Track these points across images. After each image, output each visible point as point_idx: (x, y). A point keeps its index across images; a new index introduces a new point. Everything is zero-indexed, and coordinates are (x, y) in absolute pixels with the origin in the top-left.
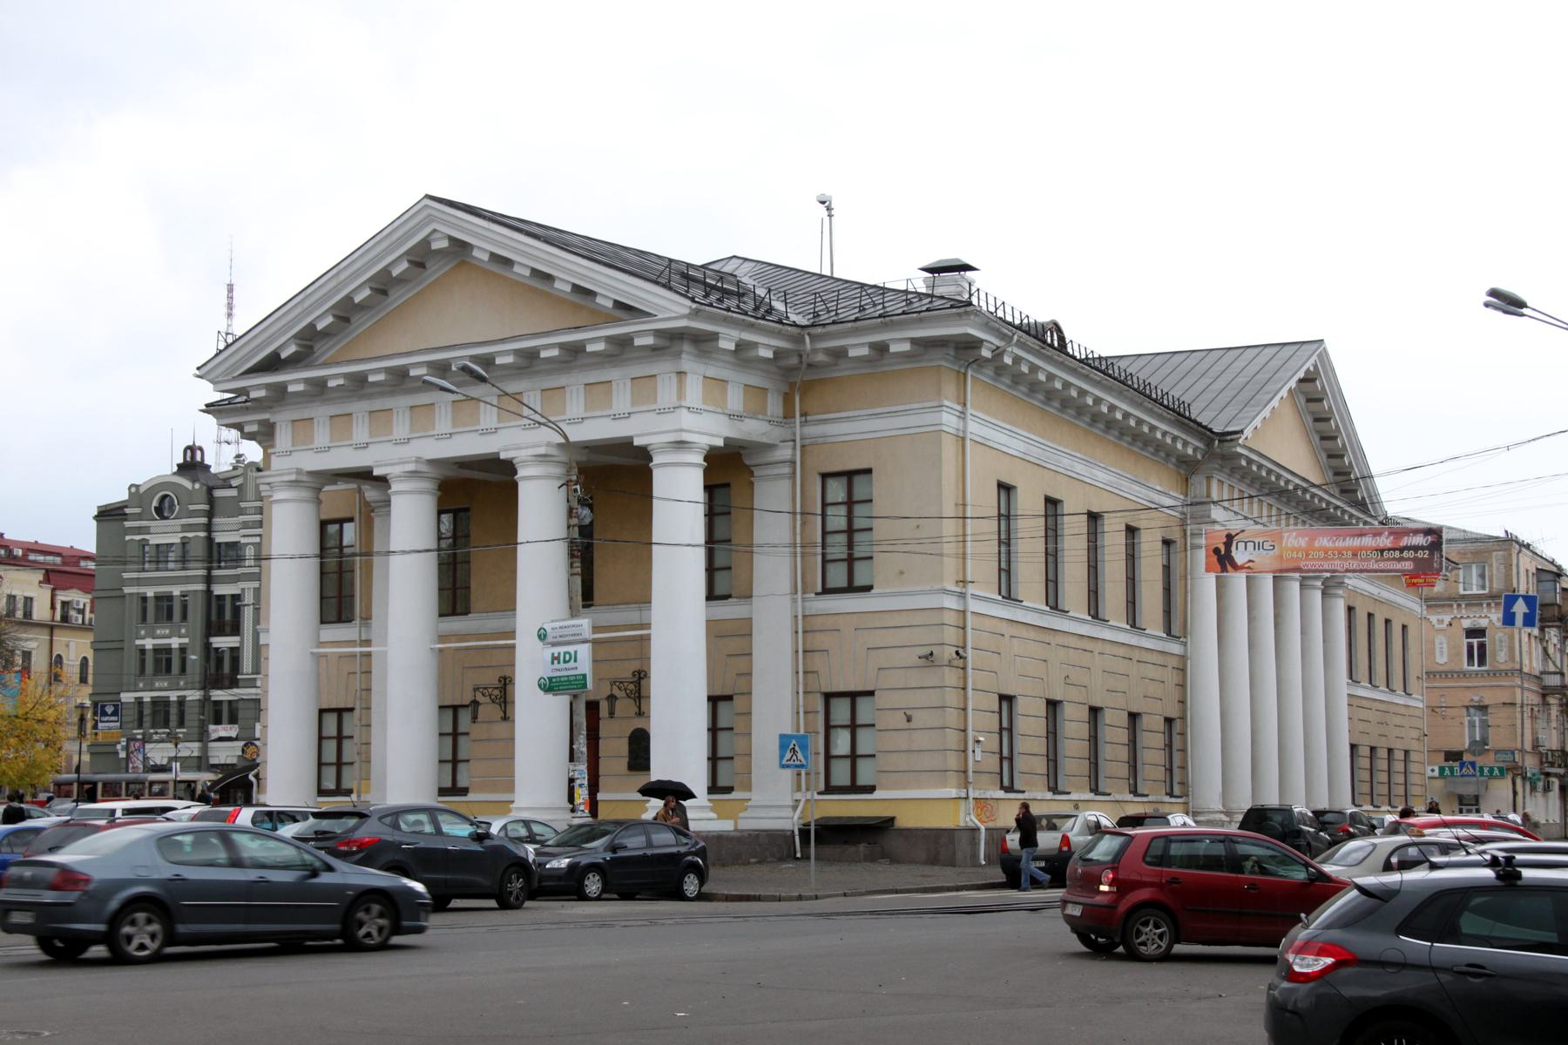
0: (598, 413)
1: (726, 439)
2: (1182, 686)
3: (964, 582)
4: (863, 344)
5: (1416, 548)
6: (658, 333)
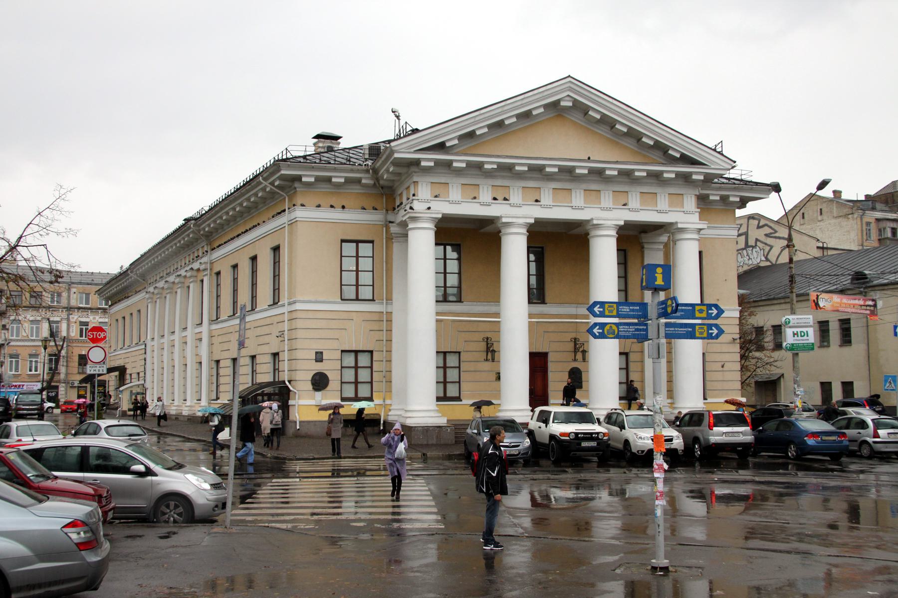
5: (870, 306)
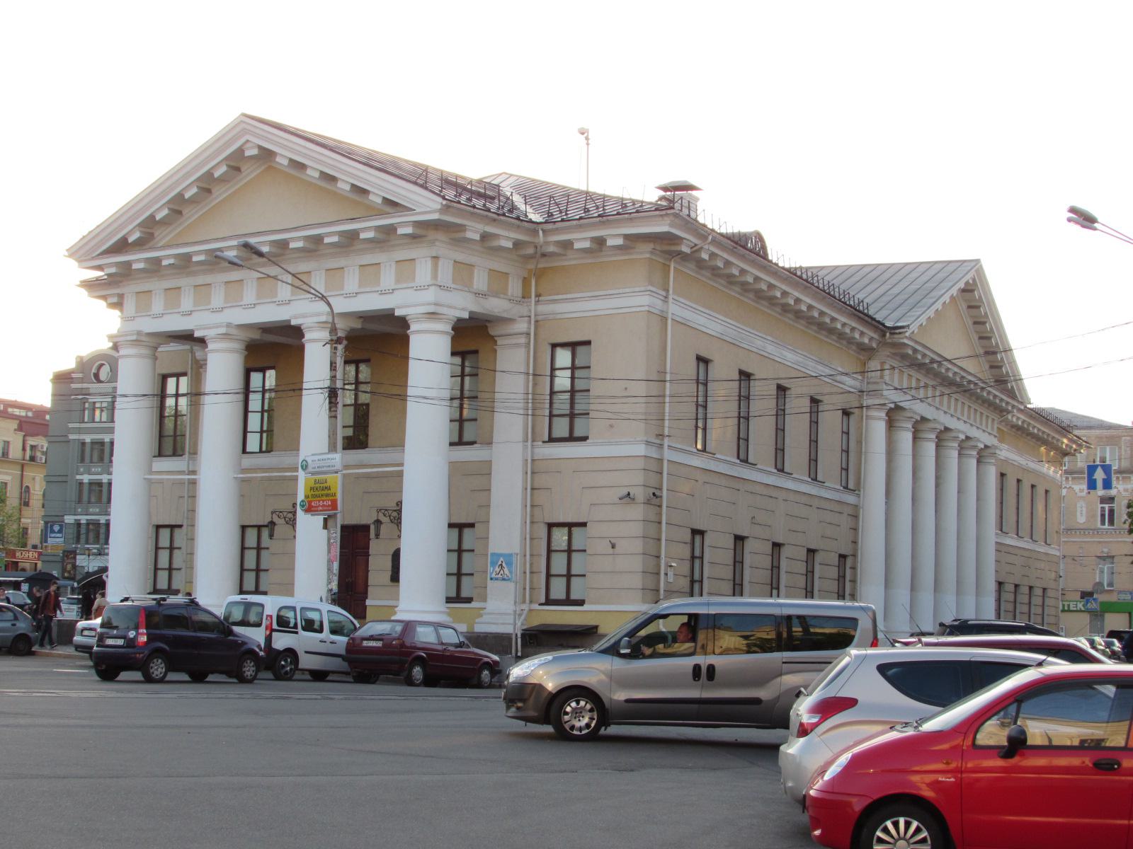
0: (368, 290)
1: (471, 313)
2: (855, 529)
3: (661, 436)
6: (418, 224)
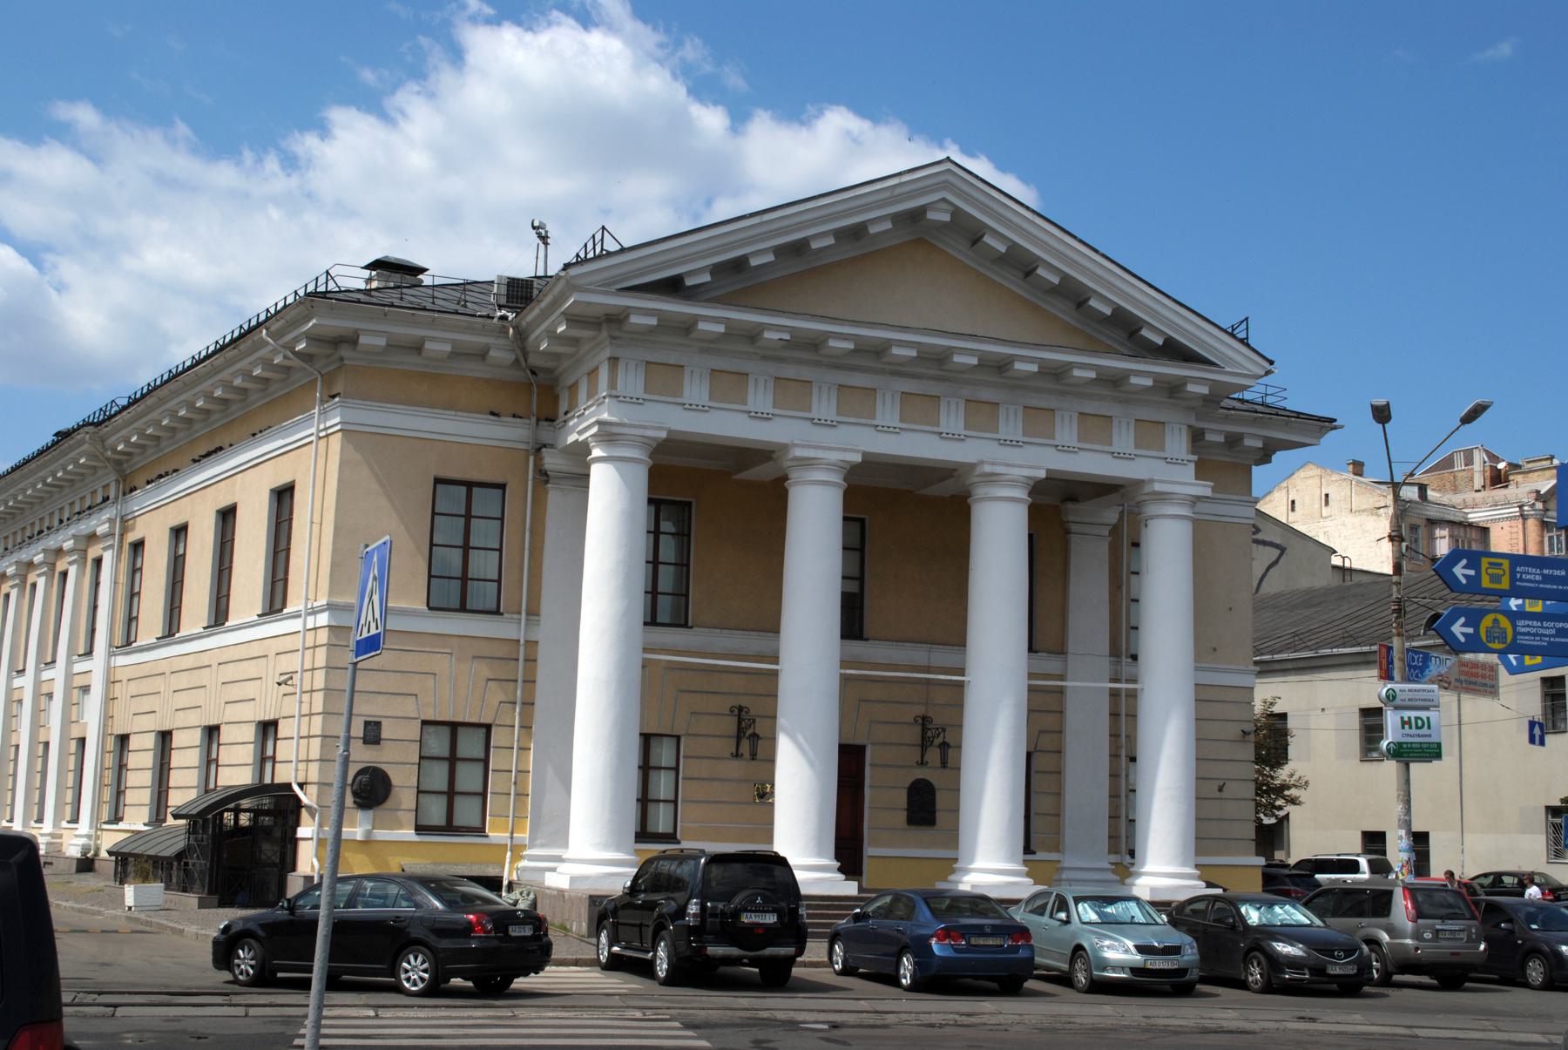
0: (1099, 447)
4: (1220, 432)
